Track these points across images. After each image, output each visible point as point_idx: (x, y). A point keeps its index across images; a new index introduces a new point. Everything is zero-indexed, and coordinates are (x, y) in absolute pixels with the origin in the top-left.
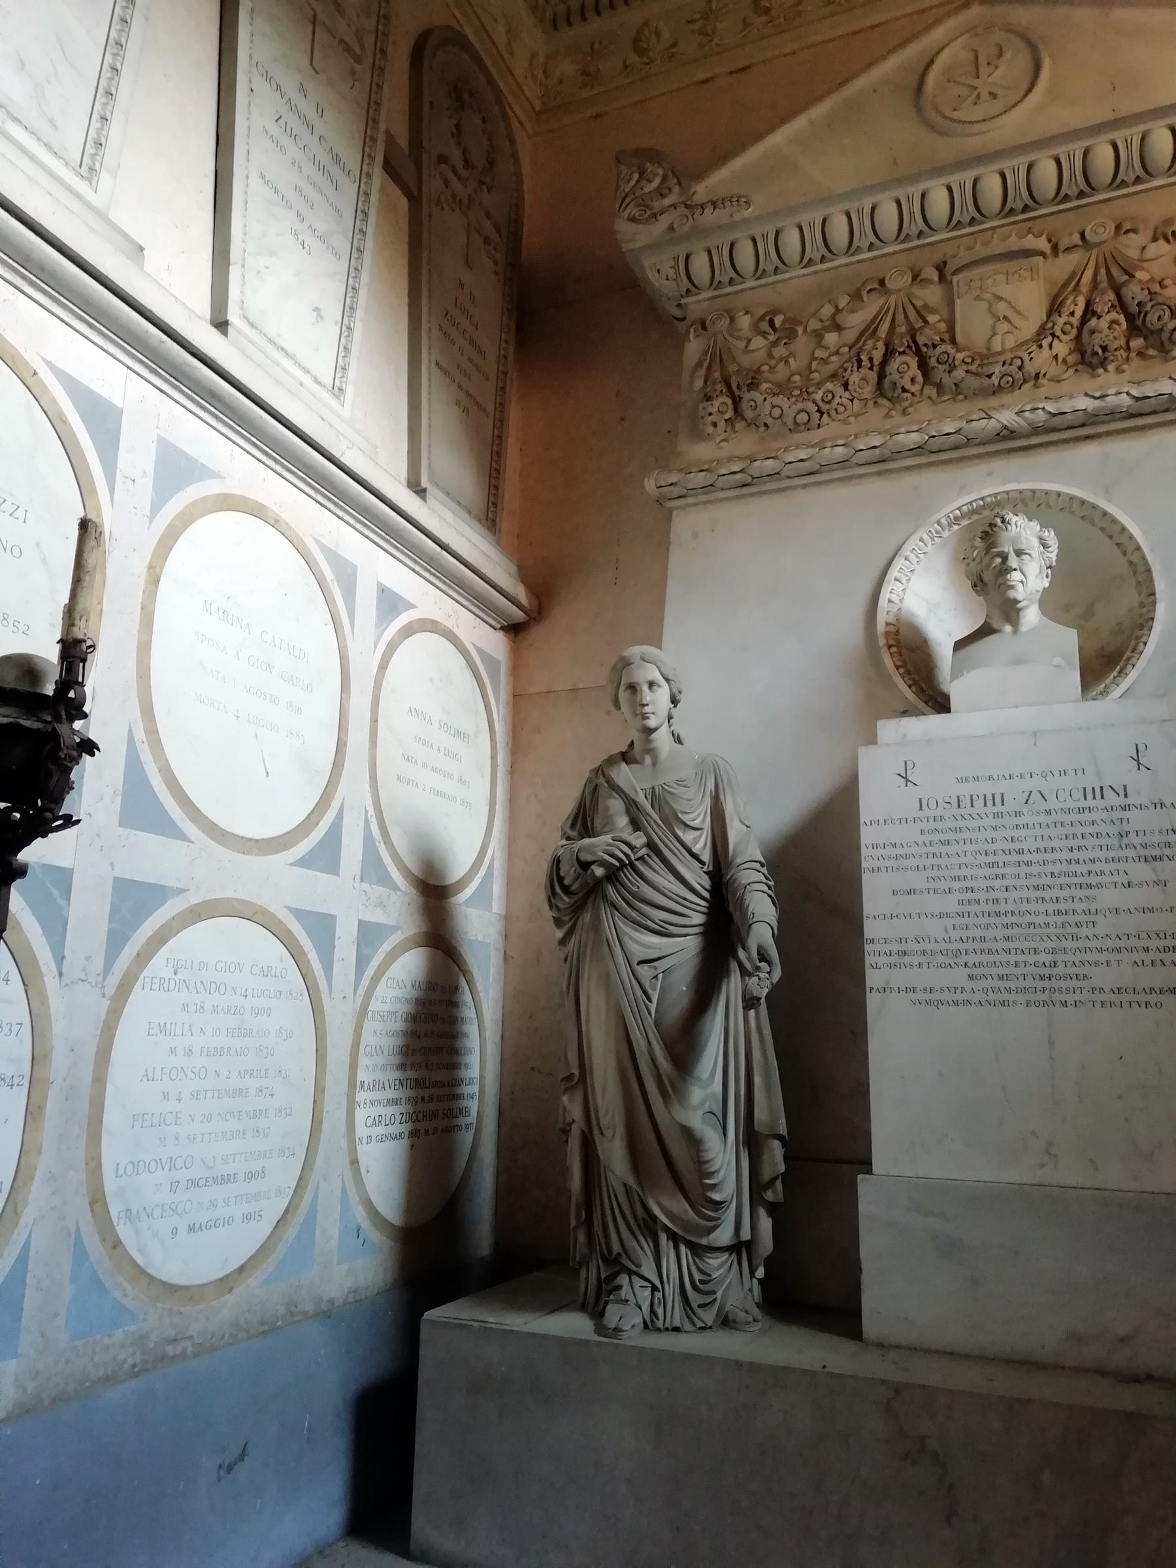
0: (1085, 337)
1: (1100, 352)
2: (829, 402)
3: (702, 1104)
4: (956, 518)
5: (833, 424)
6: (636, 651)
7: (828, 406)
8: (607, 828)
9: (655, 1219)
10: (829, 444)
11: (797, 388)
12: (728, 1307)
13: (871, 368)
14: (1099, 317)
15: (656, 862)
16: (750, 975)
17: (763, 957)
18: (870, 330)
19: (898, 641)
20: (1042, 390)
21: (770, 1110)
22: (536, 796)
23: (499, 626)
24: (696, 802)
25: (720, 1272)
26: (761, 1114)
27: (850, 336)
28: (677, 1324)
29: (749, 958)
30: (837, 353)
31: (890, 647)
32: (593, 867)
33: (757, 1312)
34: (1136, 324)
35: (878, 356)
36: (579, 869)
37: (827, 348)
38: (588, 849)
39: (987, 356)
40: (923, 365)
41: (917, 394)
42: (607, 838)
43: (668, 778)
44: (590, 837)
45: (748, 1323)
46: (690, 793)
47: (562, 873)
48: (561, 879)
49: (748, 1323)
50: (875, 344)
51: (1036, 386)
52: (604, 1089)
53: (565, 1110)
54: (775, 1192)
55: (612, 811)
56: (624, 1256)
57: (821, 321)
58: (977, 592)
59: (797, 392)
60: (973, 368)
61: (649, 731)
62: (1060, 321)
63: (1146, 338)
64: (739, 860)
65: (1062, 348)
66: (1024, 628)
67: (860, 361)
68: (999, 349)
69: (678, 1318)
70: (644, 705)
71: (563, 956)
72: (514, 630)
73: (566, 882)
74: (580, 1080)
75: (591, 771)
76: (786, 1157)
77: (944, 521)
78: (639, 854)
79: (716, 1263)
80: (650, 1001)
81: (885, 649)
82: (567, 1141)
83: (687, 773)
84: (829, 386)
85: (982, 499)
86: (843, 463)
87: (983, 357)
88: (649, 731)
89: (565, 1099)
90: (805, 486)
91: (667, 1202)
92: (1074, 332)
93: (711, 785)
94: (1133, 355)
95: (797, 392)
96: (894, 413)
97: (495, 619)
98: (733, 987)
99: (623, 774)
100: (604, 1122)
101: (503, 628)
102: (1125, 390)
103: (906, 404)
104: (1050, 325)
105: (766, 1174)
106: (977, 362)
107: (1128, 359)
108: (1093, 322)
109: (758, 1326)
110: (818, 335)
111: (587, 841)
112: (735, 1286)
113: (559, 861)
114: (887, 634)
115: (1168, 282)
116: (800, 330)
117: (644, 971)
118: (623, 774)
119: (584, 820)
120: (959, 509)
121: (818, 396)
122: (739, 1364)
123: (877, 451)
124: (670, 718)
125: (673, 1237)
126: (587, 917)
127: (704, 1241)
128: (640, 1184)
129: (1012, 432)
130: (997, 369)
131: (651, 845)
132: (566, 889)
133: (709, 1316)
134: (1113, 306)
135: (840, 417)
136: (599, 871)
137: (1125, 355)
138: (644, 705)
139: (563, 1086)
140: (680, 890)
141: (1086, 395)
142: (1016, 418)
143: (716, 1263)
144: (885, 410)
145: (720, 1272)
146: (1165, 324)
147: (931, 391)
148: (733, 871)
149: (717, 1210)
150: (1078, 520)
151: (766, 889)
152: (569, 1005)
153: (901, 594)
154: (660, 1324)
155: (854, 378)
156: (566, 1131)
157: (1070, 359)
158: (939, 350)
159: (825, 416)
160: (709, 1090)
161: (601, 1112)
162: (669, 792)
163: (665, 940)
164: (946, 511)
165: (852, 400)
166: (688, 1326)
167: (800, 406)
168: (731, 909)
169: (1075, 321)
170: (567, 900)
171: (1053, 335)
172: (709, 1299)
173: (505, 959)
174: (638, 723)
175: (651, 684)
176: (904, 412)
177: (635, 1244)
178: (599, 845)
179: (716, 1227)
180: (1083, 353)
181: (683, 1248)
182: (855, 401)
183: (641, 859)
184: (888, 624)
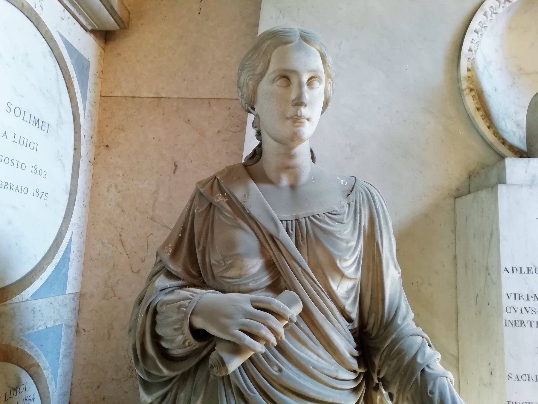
22: (116, 187)
55: (241, 249)
93: (365, 221)
97: (86, 19)
170: (166, 372)
173: (77, 332)
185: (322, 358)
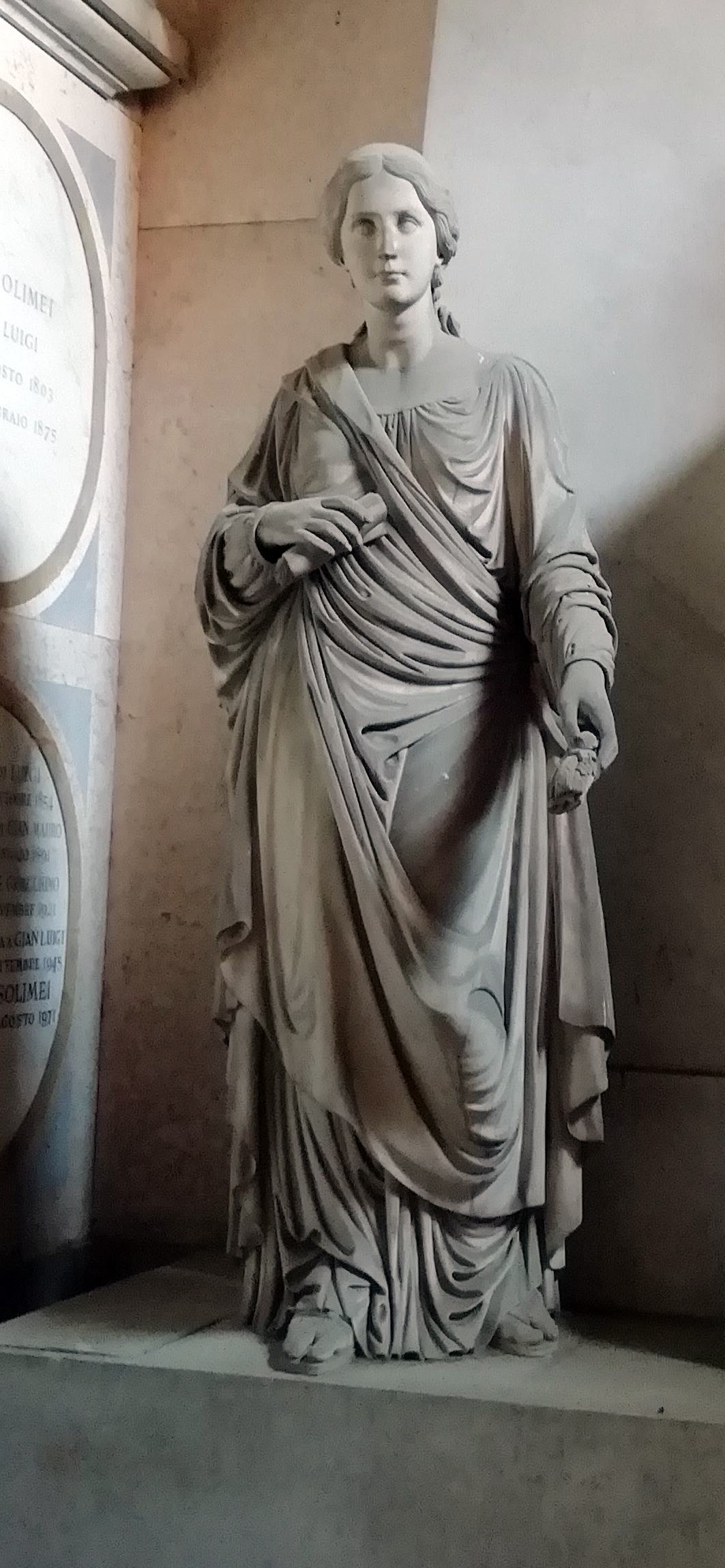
3: (470, 974)
6: (376, 152)
8: (314, 485)
9: (378, 1171)
12: (501, 1318)
15: (402, 551)
16: (562, 754)
17: (587, 723)
21: (587, 987)
23: (111, 92)
24: (479, 443)
25: (490, 1259)
26: (570, 992)
28: (413, 1346)
29: (564, 727)
32: (287, 555)
33: (552, 1327)
36: (260, 559)
38: (279, 522)
42: (313, 503)
43: (428, 395)
44: (282, 500)
45: (534, 1344)
46: (466, 426)
47: (228, 566)
48: (225, 576)
49: (534, 1344)
52: (297, 952)
53: (224, 986)
54: (590, 1125)
56: (324, 1236)
61: (396, 307)
64: (551, 551)
69: (415, 1336)
70: (388, 257)
71: (227, 717)
72: (141, 101)
73: (236, 582)
74: (254, 934)
75: (286, 379)
76: (611, 1067)
78: (372, 535)
79: (484, 1246)
80: (383, 795)
82: (227, 1041)
83: (464, 388)
88: (396, 307)
89: (226, 967)
91: (403, 1144)
98: (531, 775)
99: (344, 386)
100: (294, 1007)
101: (121, 97)
105: (576, 1096)
109: (554, 1346)
111: (276, 507)
112: (514, 1281)
113: (222, 543)
117: (376, 745)
118: (344, 386)
119: (269, 472)
122: (516, 1411)
124: (435, 284)
125: (412, 1202)
126: (273, 646)
127: (464, 1208)
128: (355, 1109)
131: (394, 519)
132: (235, 595)
133: (468, 1334)
136: (298, 564)
138: (388, 257)
139: (222, 945)
140: (441, 604)
143: (484, 1246)
145: (490, 1259)
148: (539, 570)
149: (488, 1155)
151: (596, 602)
152: (237, 802)
154: (383, 1348)
156: (225, 1023)
160: (482, 952)
161: (290, 990)
162: (430, 423)
163: (414, 690)
166: (431, 1350)
168: (534, 637)
170: (236, 613)
172: (470, 1305)
174: (372, 291)
175: (403, 218)
177: (344, 1215)
178: (298, 516)
179: (484, 1185)
181: (427, 1221)
183: (375, 543)
185: (431, 590)
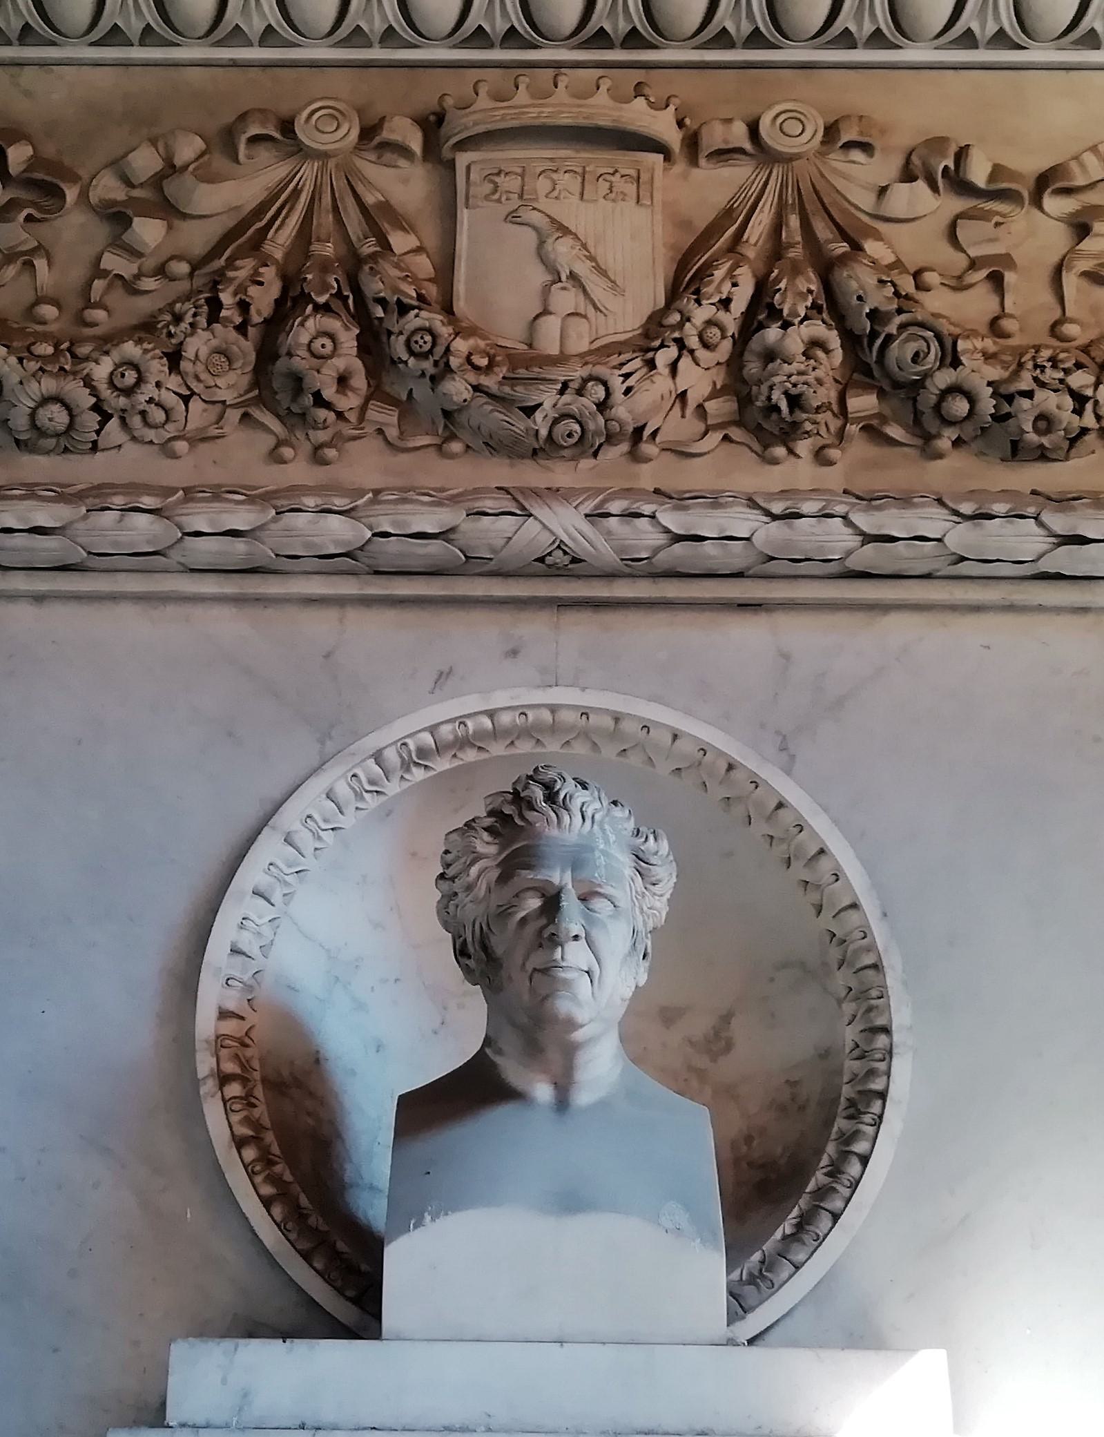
0: (753, 367)
1: (784, 405)
2: (128, 392)
4: (422, 752)
5: (131, 449)
7: (122, 402)
10: (119, 500)
11: (45, 337)
13: (242, 329)
14: (786, 325)
18: (246, 234)
19: (245, 1065)
20: (645, 467)
27: (197, 237)
30: (161, 271)
31: (224, 1079)
34: (864, 355)
35: (264, 299)
37: (134, 253)
39: (526, 363)
40: (372, 344)
41: (352, 417)
50: (256, 272)
51: (635, 456)
57: (129, 184)
58: (468, 972)
59: (46, 349)
60: (490, 382)
62: (700, 315)
63: (882, 394)
65: (697, 379)
66: (583, 1097)
67: (215, 305)
68: (555, 351)
77: (391, 756)
81: (209, 1087)
84: (130, 349)
85: (491, 714)
86: (148, 559)
87: (514, 360)
90: (39, 598)
92: (727, 345)
94: (853, 429)
95: (46, 349)
96: (287, 452)
102: (840, 509)
103: (322, 436)
104: (675, 318)
106: (502, 371)
107: (841, 435)
108: (773, 333)
110: (118, 218)
114: (220, 1041)
115: (931, 278)
116: (71, 194)
120: (432, 729)
121: (102, 370)
123: (240, 546)
129: (575, 560)
130: (548, 398)
134: (816, 307)
135: (151, 434)
137: (835, 424)
141: (752, 503)
142: (585, 526)
144: (271, 441)
146: (927, 375)
147: (386, 417)
150: (728, 824)
153: (267, 931)
155: (198, 345)
157: (711, 406)
158: (413, 320)
159: (114, 423)
164: (399, 729)
165: (186, 400)
167: (49, 385)
169: (731, 321)
171: (681, 343)
176: (317, 457)
180: (745, 401)
182: (195, 404)
184: (224, 1014)
